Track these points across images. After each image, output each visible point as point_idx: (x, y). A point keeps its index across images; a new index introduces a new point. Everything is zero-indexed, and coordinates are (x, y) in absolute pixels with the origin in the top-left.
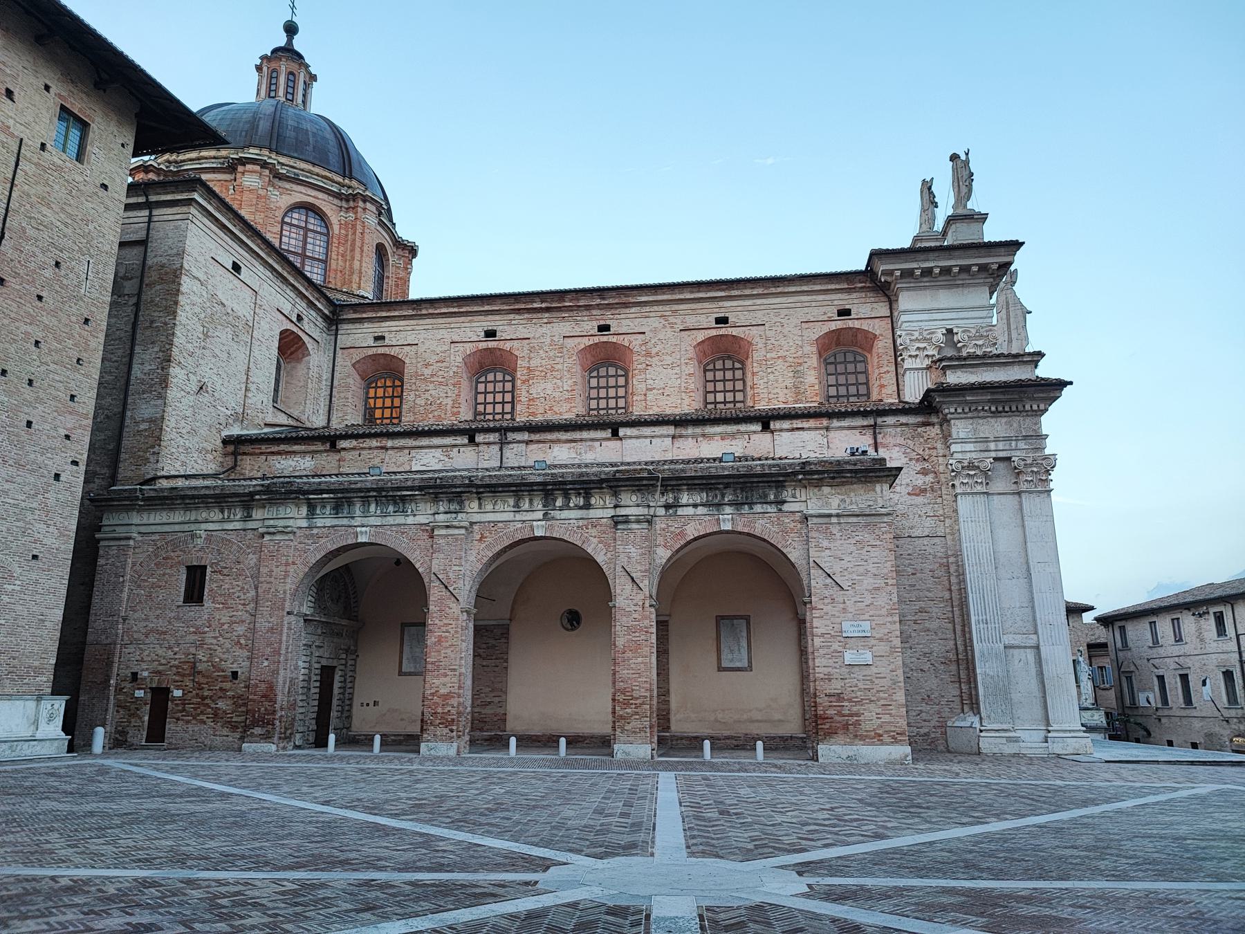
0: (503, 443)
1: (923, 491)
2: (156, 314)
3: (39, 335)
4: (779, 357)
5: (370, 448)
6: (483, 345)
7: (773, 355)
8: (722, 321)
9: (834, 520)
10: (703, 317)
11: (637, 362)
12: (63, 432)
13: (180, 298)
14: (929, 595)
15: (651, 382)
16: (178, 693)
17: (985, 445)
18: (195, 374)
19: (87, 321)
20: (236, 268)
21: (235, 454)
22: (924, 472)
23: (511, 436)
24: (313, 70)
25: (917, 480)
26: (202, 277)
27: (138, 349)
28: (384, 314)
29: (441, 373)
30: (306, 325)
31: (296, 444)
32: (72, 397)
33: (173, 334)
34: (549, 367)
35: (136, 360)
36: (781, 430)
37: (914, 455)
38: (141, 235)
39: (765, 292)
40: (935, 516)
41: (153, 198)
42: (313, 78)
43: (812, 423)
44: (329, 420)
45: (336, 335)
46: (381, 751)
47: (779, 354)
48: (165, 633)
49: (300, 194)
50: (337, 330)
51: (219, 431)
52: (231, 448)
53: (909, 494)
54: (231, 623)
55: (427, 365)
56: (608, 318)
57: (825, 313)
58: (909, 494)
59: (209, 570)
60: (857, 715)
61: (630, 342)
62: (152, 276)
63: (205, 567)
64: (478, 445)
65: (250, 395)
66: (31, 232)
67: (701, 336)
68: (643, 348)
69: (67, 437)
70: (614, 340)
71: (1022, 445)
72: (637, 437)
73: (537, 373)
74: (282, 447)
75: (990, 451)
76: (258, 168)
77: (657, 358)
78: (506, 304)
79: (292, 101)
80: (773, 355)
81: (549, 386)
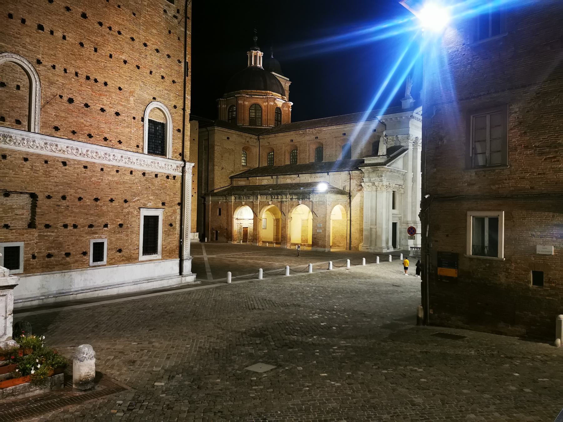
13: (215, 151)
16: (219, 232)
20: (228, 138)
26: (219, 144)
27: (209, 163)
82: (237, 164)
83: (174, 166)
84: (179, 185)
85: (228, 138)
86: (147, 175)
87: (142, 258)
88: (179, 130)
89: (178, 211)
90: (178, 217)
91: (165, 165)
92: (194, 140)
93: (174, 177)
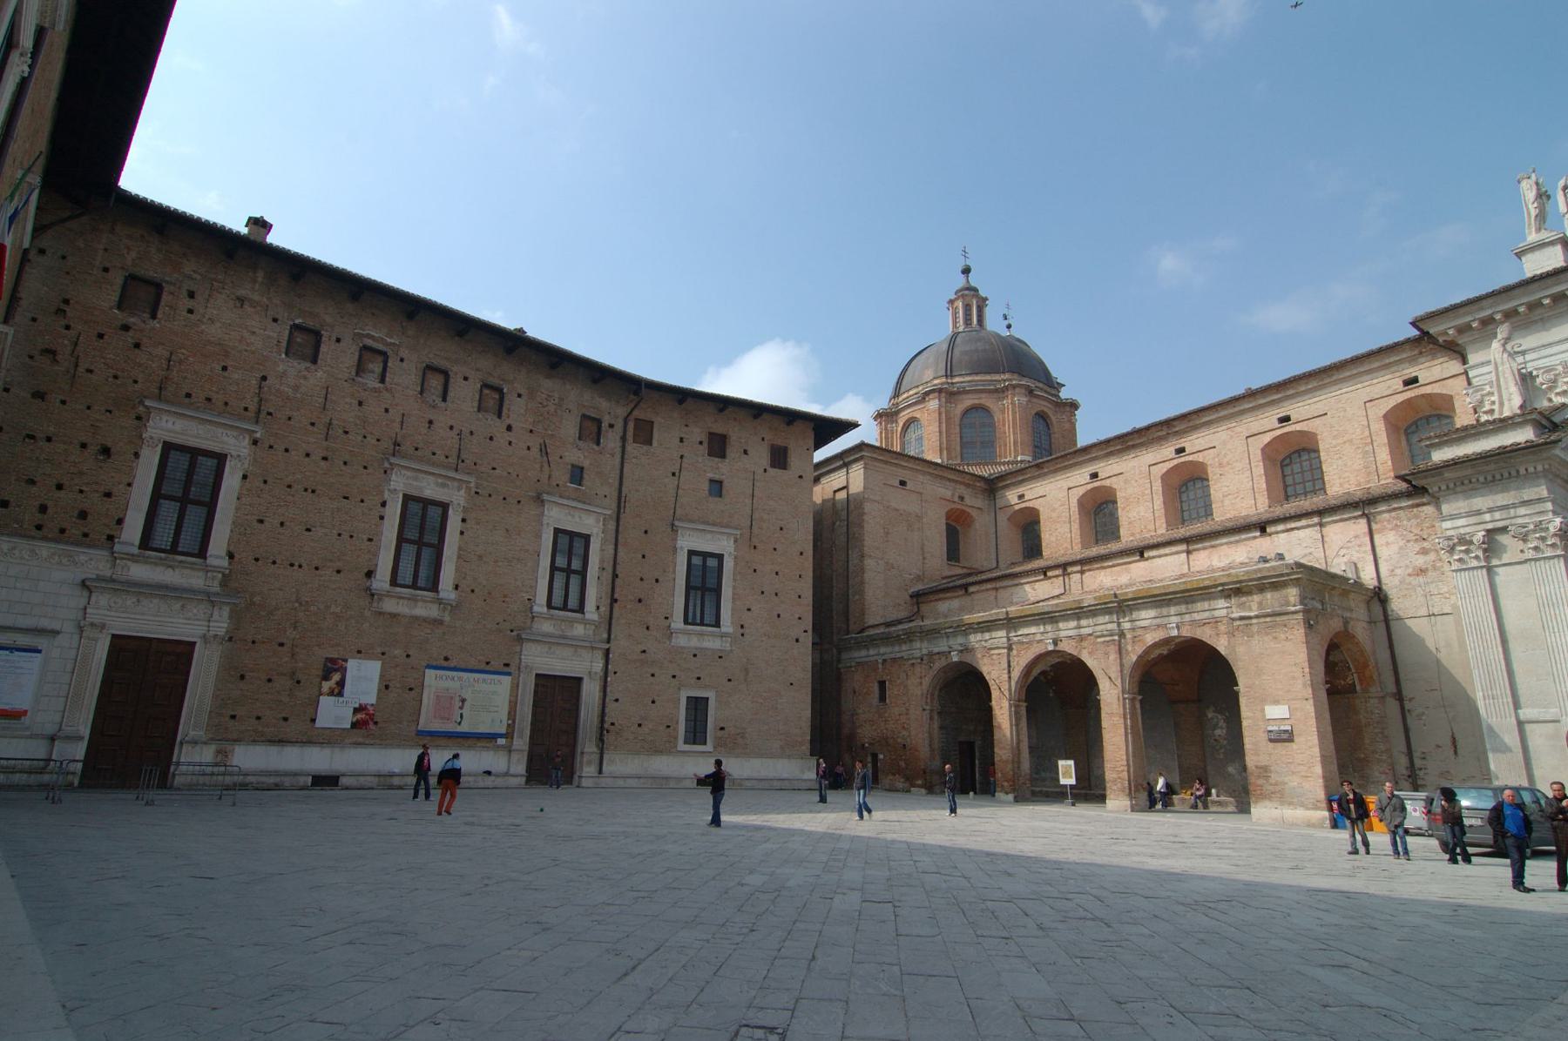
2: (855, 530)
3: (777, 569)
4: (1345, 442)
5: (987, 590)
6: (1089, 487)
7: (1340, 441)
8: (1285, 420)
9: (1254, 621)
10: (1265, 423)
11: (1212, 473)
12: (797, 616)
17: (1478, 517)
18: (882, 559)
19: (801, 554)
21: (918, 603)
22: (1424, 552)
23: (1070, 569)
24: (982, 293)
25: (1417, 560)
26: (877, 498)
27: (850, 552)
28: (1020, 478)
30: (968, 501)
31: (948, 592)
32: (800, 597)
36: (1277, 533)
37: (1411, 536)
38: (845, 484)
39: (1320, 383)
40: (1439, 594)
41: (846, 460)
42: (986, 299)
43: (1303, 522)
44: (998, 562)
45: (995, 499)
47: (1345, 439)
49: (969, 401)
50: (995, 496)
51: (906, 590)
52: (915, 600)
53: (1409, 575)
54: (900, 715)
56: (1181, 443)
58: (1409, 575)
62: (852, 507)
63: (885, 682)
64: (1050, 578)
65: (926, 561)
66: (765, 517)
67: (1267, 438)
68: (1217, 460)
69: (800, 618)
70: (1190, 459)
71: (1522, 511)
72: (1160, 556)
73: (1131, 500)
74: (941, 596)
75: (1486, 522)
76: (936, 394)
78: (1102, 450)
79: (971, 324)
80: (1340, 441)
81: (1142, 508)
85: (903, 483)
92: (801, 477)
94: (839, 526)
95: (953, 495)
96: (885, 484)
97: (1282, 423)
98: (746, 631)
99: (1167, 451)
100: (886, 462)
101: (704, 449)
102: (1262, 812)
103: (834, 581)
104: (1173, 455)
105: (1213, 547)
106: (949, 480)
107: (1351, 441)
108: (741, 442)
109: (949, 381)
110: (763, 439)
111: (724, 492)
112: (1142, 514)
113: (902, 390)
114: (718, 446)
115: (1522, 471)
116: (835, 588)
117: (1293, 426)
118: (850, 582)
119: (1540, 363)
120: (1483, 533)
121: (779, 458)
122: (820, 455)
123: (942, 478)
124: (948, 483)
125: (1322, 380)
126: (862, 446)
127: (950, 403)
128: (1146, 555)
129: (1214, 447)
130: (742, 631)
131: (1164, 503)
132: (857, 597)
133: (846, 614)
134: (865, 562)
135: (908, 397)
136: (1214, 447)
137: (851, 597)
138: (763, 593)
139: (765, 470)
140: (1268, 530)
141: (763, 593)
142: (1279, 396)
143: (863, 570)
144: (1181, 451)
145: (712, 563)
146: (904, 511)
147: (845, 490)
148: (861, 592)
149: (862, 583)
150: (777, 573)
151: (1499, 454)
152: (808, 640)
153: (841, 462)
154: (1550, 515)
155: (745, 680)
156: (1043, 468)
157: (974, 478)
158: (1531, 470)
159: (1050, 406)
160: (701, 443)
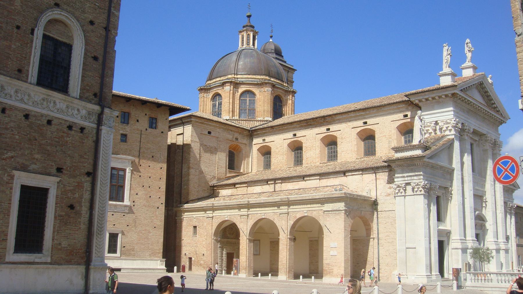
0: (275, 183)
1: (389, 195)
2: (186, 155)
3: (150, 175)
7: (382, 135)
11: (339, 141)
14: (390, 230)
15: (343, 149)
19: (161, 168)
27: (183, 165)
29: (281, 151)
32: (160, 188)
33: (190, 160)
34: (312, 146)
35: (183, 169)
36: (349, 175)
41: (183, 121)
46: (302, 280)
48: (190, 243)
53: (385, 196)
54: (202, 241)
55: (277, 148)
56: (330, 127)
57: (399, 117)
58: (385, 196)
59: (197, 227)
60: (333, 269)
61: (336, 134)
64: (269, 184)
67: (359, 130)
69: (159, 198)
72: (310, 180)
77: (344, 139)
79: (249, 45)
80: (382, 135)
82: (221, 167)
83: (84, 112)
84: (89, 143)
85: (209, 133)
86: (32, 119)
87: (12, 257)
88: (95, 58)
89: (87, 186)
90: (87, 196)
91: (67, 107)
92: (162, 132)
93: (82, 129)
94: (179, 151)
95: (233, 137)
96: (201, 133)
97: (364, 124)
98: (135, 204)
99: (323, 129)
100: (202, 123)
101: (119, 120)
102: (326, 280)
103: (175, 178)
104: (325, 131)
105: (328, 178)
106: (231, 131)
107: (385, 136)
108: (136, 117)
109: (236, 76)
110: (146, 115)
111: (127, 140)
112: (312, 155)
113: (213, 77)
114: (125, 118)
115: (416, 164)
116: (175, 181)
117: (368, 126)
118: (182, 180)
119: (441, 118)
120: (404, 184)
121: (153, 123)
122: (172, 118)
123: (228, 130)
124: (231, 132)
125: (378, 110)
126: (190, 116)
127: (235, 88)
128: (305, 179)
129: (340, 130)
130: (134, 204)
131: (320, 151)
132: (185, 187)
133: (180, 194)
134: (190, 171)
135: (215, 82)
136: (340, 130)
137: (182, 186)
138: (143, 186)
139: (146, 129)
140: (346, 174)
141: (143, 186)
142: (364, 113)
143: (188, 174)
144: (328, 129)
145: (121, 173)
146: (209, 146)
147: (182, 135)
148: (188, 185)
149: (188, 180)
150: (150, 177)
151: (409, 158)
152: (163, 208)
153: (181, 122)
154: (422, 180)
155: (135, 225)
156: (274, 129)
157: (243, 130)
158: (418, 164)
159: (283, 92)
160: (117, 117)
